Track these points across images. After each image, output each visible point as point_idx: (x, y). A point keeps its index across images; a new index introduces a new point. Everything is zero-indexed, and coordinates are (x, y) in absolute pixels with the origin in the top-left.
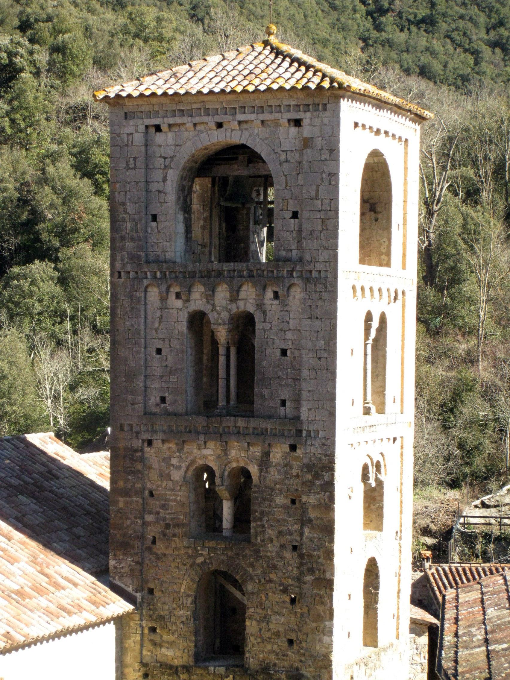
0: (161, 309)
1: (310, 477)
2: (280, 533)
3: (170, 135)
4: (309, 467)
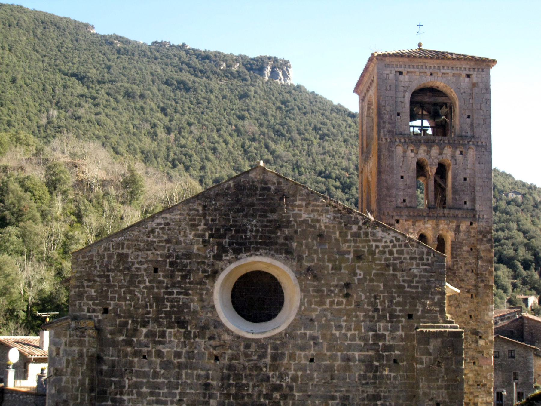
0: (403, 157)
1: (481, 237)
2: (466, 264)
3: (407, 77)
4: (480, 232)
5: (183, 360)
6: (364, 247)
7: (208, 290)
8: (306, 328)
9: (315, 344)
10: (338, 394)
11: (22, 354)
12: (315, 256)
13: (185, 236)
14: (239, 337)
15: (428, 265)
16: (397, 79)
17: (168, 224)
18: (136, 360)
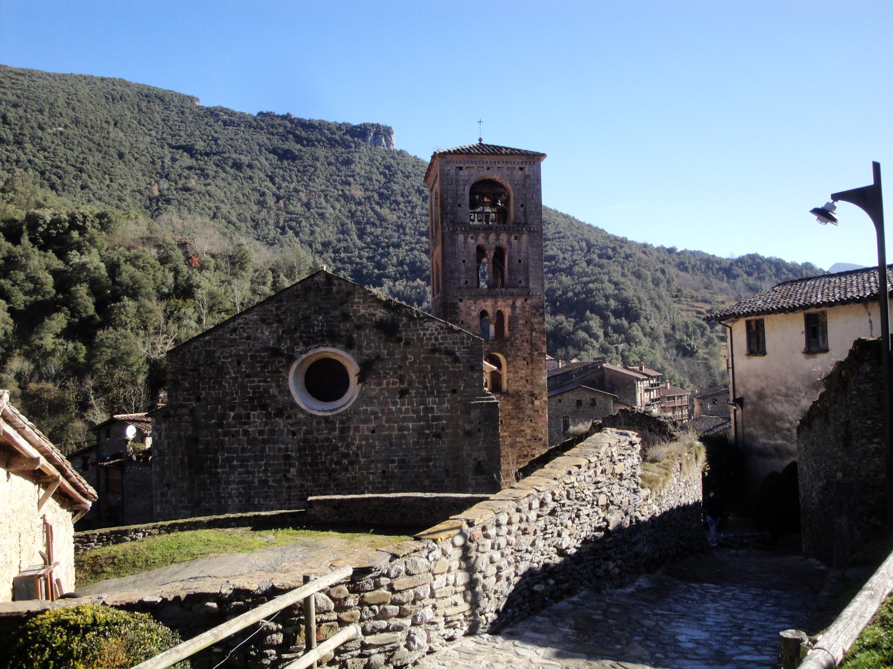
4: (534, 307)
5: (266, 437)
6: (413, 335)
7: (283, 377)
8: (367, 406)
9: (376, 418)
10: (396, 458)
11: (138, 430)
12: (373, 345)
13: (262, 333)
14: (311, 415)
15: (469, 348)
16: (457, 175)
17: (247, 324)
18: (227, 439)
